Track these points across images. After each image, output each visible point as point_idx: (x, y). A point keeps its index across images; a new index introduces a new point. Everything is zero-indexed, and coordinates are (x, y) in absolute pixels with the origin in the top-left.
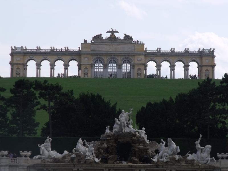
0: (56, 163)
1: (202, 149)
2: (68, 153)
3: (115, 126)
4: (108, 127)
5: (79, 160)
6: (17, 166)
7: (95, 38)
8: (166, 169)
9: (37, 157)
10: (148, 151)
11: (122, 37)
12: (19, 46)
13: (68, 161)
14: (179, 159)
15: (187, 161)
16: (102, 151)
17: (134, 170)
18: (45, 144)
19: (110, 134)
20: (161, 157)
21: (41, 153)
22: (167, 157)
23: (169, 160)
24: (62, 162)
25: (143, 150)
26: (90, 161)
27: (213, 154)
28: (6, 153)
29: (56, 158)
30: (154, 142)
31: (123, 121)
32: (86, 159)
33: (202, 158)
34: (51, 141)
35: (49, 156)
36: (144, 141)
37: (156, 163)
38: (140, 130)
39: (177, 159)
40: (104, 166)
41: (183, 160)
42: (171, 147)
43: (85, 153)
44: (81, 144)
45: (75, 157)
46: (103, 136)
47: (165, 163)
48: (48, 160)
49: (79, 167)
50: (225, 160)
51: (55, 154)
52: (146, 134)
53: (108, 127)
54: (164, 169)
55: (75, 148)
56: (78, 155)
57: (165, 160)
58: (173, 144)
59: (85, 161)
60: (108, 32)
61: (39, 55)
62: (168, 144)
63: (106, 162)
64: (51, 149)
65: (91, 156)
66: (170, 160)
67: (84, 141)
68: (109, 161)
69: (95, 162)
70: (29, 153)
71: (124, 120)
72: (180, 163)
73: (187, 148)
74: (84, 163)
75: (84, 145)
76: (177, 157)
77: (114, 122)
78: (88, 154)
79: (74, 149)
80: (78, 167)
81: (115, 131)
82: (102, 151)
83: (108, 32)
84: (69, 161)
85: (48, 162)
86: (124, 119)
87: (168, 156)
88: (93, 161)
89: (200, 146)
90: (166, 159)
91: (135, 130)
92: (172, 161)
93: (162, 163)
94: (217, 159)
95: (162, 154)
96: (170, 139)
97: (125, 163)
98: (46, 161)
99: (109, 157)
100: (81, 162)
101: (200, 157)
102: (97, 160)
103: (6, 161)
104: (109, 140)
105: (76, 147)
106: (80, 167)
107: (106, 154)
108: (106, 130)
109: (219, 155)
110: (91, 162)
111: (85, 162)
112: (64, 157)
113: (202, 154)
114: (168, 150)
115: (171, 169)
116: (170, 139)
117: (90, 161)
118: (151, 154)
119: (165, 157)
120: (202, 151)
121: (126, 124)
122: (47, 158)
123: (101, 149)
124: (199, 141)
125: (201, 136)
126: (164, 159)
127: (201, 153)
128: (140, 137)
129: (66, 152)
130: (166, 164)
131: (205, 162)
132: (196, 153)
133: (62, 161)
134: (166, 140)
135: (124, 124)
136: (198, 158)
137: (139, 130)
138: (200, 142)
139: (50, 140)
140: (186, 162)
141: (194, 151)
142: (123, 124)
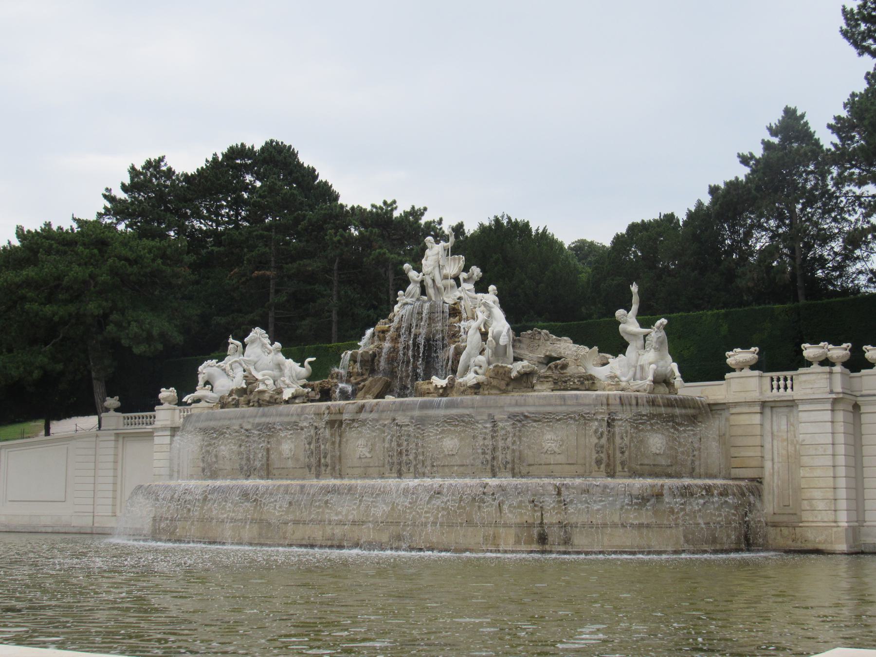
1: (645, 336)
22: (480, 367)
26: (266, 397)
38: (480, 295)
50: (747, 372)
57: (471, 378)
69: (287, 402)
71: (430, 265)
72: (533, 387)
74: (256, 404)
87: (485, 365)
92: (495, 382)
93: (462, 389)
115: (491, 411)
119: (477, 368)
124: (635, 307)
125: (634, 288)
127: (641, 352)
132: (624, 354)
135: (433, 281)
138: (639, 310)
140: (555, 383)
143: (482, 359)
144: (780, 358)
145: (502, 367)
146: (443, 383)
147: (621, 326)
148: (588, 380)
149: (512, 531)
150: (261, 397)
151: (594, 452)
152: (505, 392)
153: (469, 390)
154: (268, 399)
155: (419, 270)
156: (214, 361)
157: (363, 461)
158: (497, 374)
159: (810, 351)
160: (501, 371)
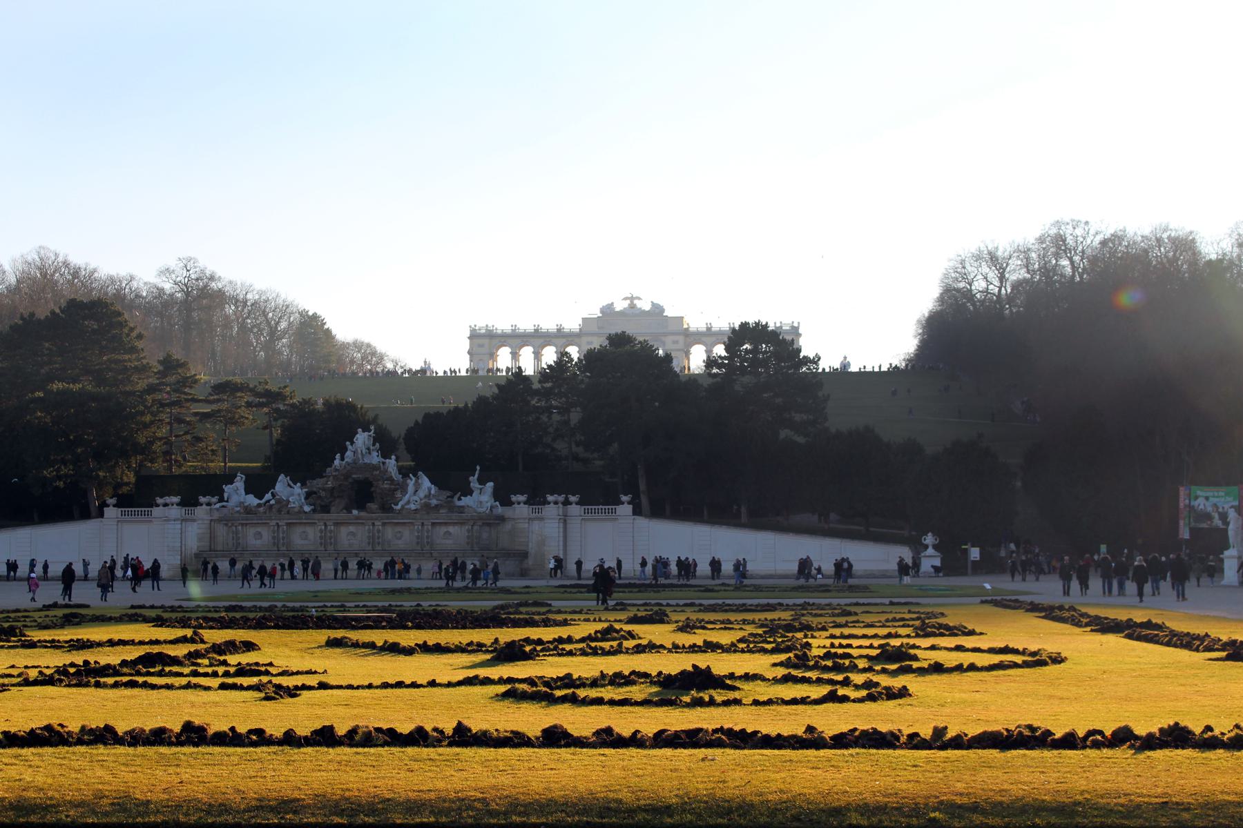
3: (349, 453)
4: (338, 456)
6: (194, 521)
7: (602, 311)
9: (218, 505)
11: (646, 307)
12: (481, 323)
20: (408, 502)
27: (502, 497)
28: (176, 499)
46: (328, 470)
51: (252, 500)
53: (338, 456)
56: (279, 501)
57: (413, 507)
60: (626, 299)
61: (517, 339)
63: (328, 512)
68: (333, 509)
70: (214, 500)
76: (434, 502)
77: (346, 450)
83: (626, 299)
89: (477, 485)
94: (506, 502)
97: (355, 512)
102: (307, 508)
103: (175, 512)
109: (514, 498)
112: (259, 505)
113: (481, 498)
114: (421, 489)
134: (415, 475)
141: (468, 492)
143: (416, 498)
144: (536, 499)
146: (399, 507)
155: (352, 443)
159: (550, 498)
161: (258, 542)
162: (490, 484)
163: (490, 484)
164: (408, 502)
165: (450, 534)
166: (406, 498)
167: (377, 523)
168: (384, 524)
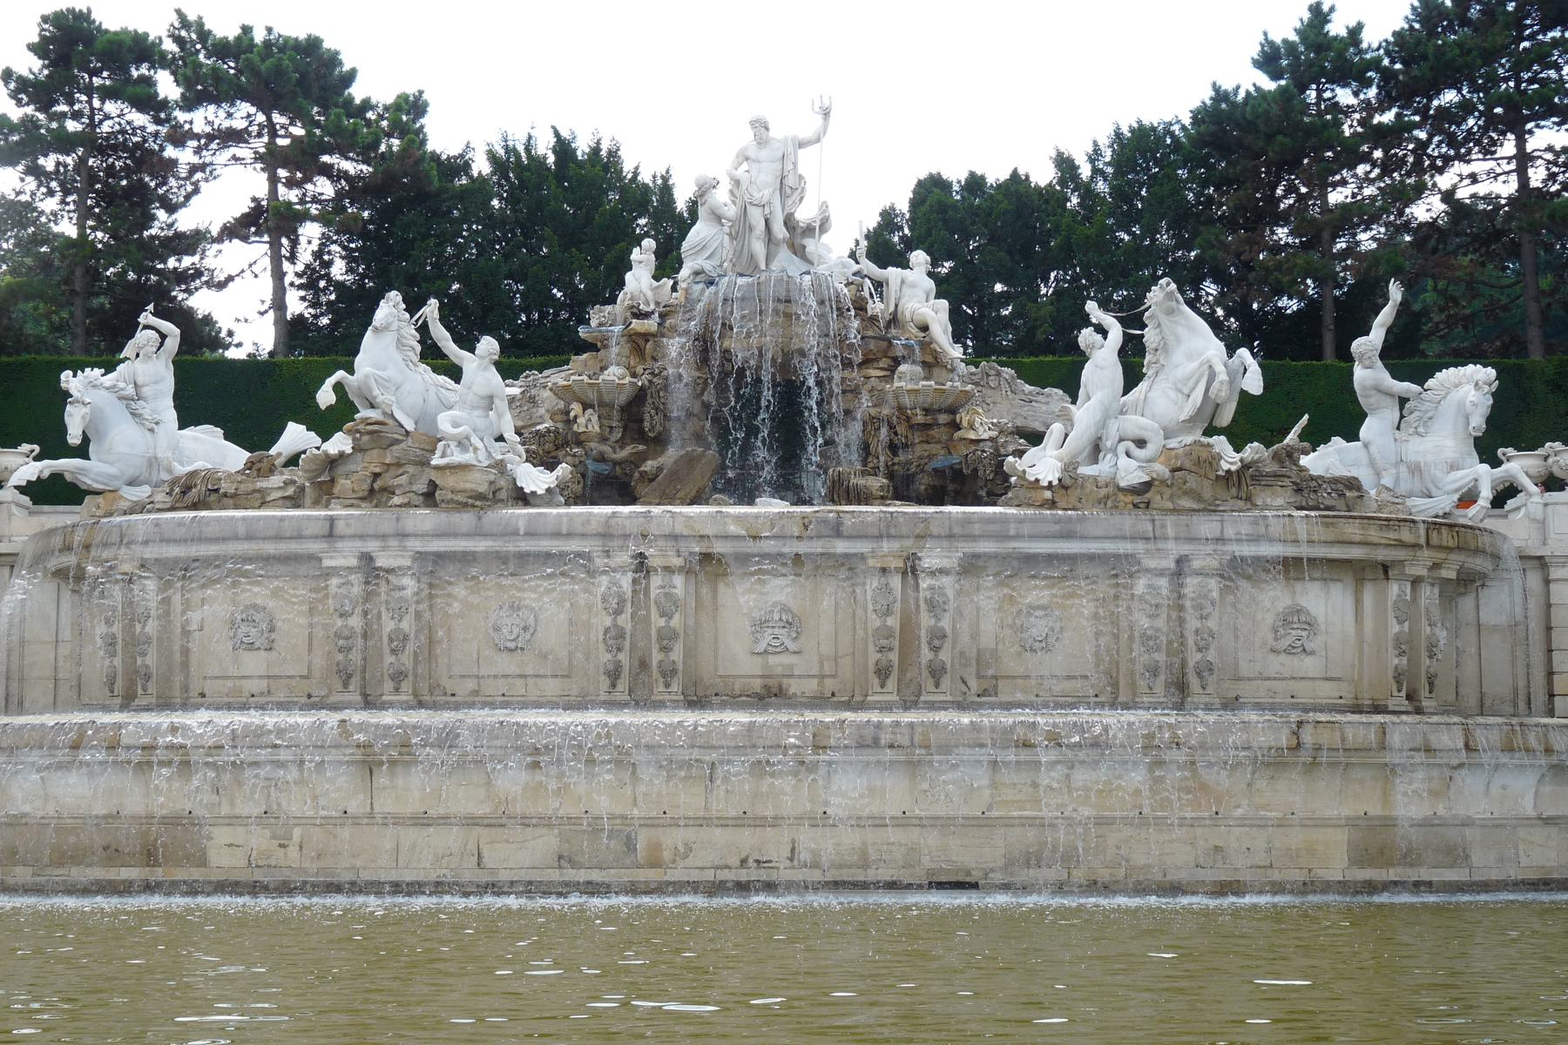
0: (195, 506)
1: (1403, 401)
2: (313, 438)
3: (698, 232)
5: (376, 476)
8: (1140, 547)
10: (964, 417)
13: (290, 491)
14: (1246, 466)
15: (1307, 490)
16: (588, 423)
17: (862, 557)
18: (120, 367)
19: (657, 304)
20: (1096, 450)
21: (74, 438)
22: (1141, 443)
23: (1168, 473)
24: (236, 500)
25: (927, 411)
26: (478, 482)
29: (193, 474)
30: (999, 374)
31: (757, 195)
32: (437, 468)
33: (1416, 470)
34: (173, 343)
35: (153, 462)
36: (926, 345)
37: (1048, 494)
38: (893, 273)
39: (1225, 466)
40: (594, 527)
41: (1276, 476)
42: (1178, 356)
43: (426, 419)
44: (400, 344)
45: (342, 455)
46: (597, 315)
47: (1129, 498)
48: (142, 493)
49: (376, 537)
51: (211, 450)
52: (938, 296)
53: (643, 256)
54: (1123, 547)
55: (340, 374)
57: (1130, 471)
58: (1192, 329)
59: (433, 486)
62: (1150, 336)
64: (172, 415)
65: (479, 444)
66: (1173, 470)
67: (425, 310)
69: (522, 498)
72: (1248, 499)
73: (1303, 387)
75: (431, 354)
76: (1230, 459)
78: (456, 425)
79: (330, 381)
80: (362, 537)
81: (697, 273)
82: (588, 423)
84: (302, 489)
85: (139, 508)
86: (762, 177)
88: (502, 483)
90: (1134, 464)
91: (856, 267)
92: (1192, 482)
93: (1103, 491)
95: (1103, 424)
96: (1173, 286)
98: (124, 505)
99: (649, 465)
100: (389, 491)
101: (1396, 465)
102: (536, 480)
104: (646, 336)
105: (351, 371)
106: (384, 537)
107: (622, 448)
108: (628, 276)
110: (480, 497)
111: (430, 497)
113: (1423, 435)
116: (1162, 293)
117: (468, 486)
118: (991, 439)
120: (1402, 417)
121: (780, 231)
122: (132, 483)
123: (586, 406)
125: (1395, 292)
126: (1123, 461)
128: (894, 320)
129: (295, 436)
130: (1136, 506)
131: (1444, 502)
132: (1352, 436)
133: (234, 496)
135: (767, 221)
136: (1378, 475)
137: (883, 265)
139: (163, 337)
140: (1299, 490)
141: (1343, 418)
142: (757, 218)
145: (1209, 445)
147: (1359, 373)
148: (1350, 489)
149: (1341, 837)
150: (448, 481)
151: (1392, 651)
152: (1210, 509)
153: (1121, 497)
154: (483, 488)
156: (98, 372)
157: (772, 660)
158: (1198, 462)
160: (1204, 455)
161: (254, 663)
162: (1467, 387)
163: (1467, 387)
164: (1096, 450)
165: (1310, 625)
166: (1085, 414)
167: (932, 558)
168: (971, 567)
